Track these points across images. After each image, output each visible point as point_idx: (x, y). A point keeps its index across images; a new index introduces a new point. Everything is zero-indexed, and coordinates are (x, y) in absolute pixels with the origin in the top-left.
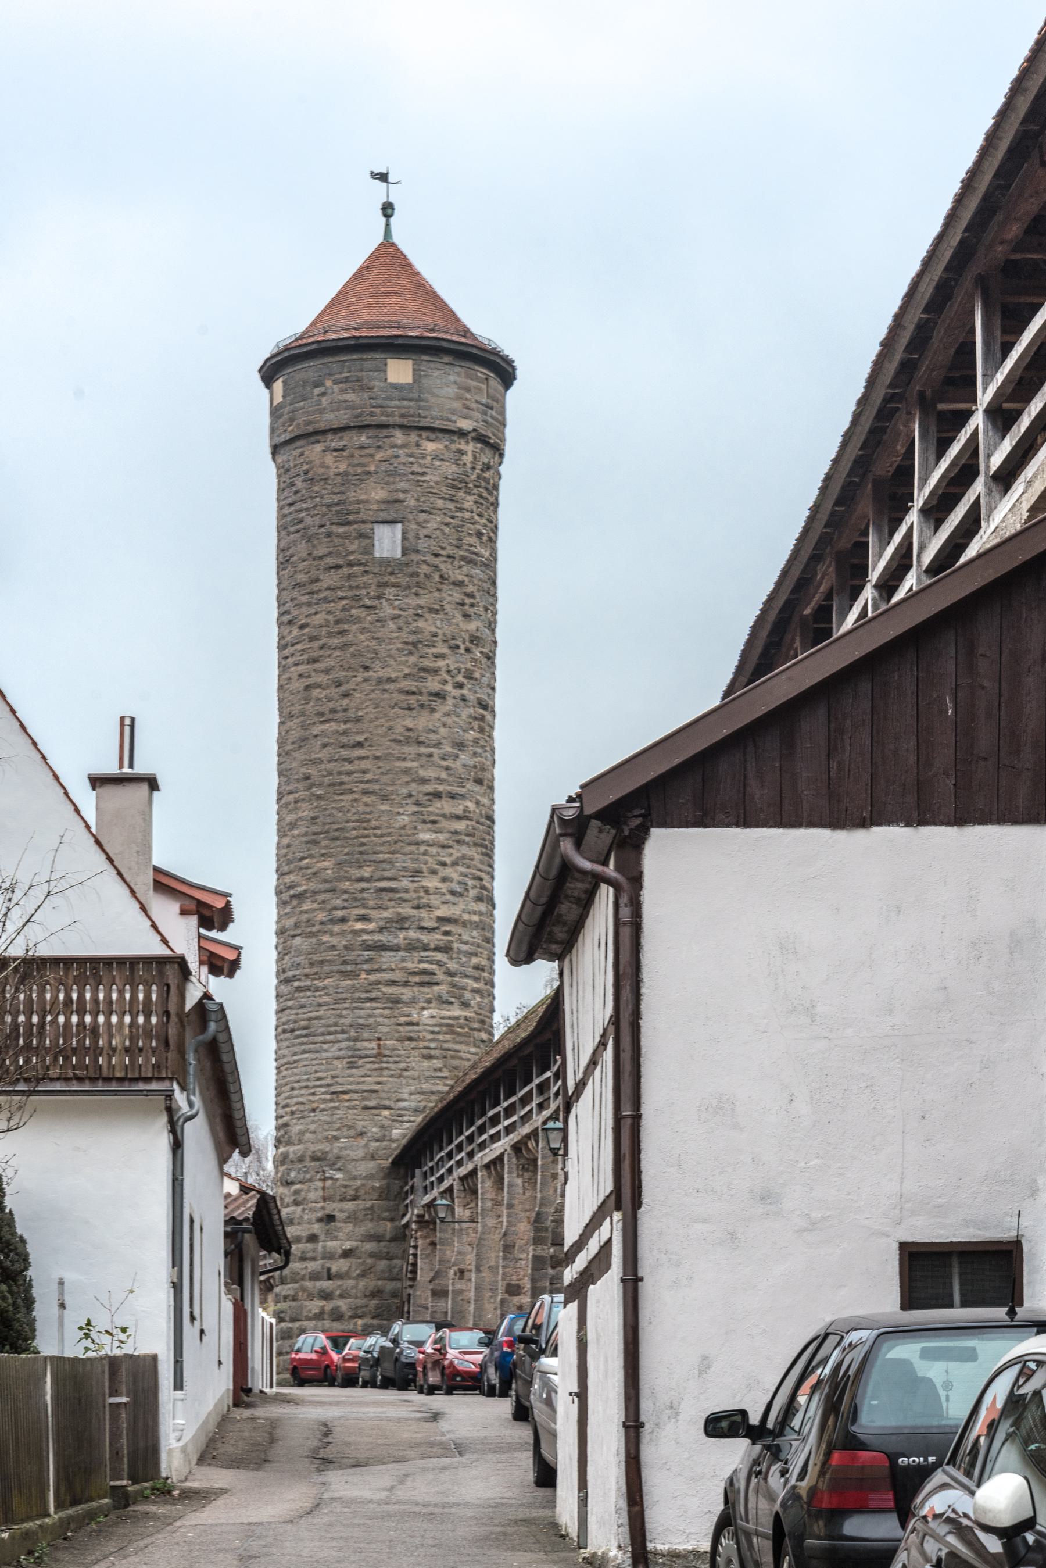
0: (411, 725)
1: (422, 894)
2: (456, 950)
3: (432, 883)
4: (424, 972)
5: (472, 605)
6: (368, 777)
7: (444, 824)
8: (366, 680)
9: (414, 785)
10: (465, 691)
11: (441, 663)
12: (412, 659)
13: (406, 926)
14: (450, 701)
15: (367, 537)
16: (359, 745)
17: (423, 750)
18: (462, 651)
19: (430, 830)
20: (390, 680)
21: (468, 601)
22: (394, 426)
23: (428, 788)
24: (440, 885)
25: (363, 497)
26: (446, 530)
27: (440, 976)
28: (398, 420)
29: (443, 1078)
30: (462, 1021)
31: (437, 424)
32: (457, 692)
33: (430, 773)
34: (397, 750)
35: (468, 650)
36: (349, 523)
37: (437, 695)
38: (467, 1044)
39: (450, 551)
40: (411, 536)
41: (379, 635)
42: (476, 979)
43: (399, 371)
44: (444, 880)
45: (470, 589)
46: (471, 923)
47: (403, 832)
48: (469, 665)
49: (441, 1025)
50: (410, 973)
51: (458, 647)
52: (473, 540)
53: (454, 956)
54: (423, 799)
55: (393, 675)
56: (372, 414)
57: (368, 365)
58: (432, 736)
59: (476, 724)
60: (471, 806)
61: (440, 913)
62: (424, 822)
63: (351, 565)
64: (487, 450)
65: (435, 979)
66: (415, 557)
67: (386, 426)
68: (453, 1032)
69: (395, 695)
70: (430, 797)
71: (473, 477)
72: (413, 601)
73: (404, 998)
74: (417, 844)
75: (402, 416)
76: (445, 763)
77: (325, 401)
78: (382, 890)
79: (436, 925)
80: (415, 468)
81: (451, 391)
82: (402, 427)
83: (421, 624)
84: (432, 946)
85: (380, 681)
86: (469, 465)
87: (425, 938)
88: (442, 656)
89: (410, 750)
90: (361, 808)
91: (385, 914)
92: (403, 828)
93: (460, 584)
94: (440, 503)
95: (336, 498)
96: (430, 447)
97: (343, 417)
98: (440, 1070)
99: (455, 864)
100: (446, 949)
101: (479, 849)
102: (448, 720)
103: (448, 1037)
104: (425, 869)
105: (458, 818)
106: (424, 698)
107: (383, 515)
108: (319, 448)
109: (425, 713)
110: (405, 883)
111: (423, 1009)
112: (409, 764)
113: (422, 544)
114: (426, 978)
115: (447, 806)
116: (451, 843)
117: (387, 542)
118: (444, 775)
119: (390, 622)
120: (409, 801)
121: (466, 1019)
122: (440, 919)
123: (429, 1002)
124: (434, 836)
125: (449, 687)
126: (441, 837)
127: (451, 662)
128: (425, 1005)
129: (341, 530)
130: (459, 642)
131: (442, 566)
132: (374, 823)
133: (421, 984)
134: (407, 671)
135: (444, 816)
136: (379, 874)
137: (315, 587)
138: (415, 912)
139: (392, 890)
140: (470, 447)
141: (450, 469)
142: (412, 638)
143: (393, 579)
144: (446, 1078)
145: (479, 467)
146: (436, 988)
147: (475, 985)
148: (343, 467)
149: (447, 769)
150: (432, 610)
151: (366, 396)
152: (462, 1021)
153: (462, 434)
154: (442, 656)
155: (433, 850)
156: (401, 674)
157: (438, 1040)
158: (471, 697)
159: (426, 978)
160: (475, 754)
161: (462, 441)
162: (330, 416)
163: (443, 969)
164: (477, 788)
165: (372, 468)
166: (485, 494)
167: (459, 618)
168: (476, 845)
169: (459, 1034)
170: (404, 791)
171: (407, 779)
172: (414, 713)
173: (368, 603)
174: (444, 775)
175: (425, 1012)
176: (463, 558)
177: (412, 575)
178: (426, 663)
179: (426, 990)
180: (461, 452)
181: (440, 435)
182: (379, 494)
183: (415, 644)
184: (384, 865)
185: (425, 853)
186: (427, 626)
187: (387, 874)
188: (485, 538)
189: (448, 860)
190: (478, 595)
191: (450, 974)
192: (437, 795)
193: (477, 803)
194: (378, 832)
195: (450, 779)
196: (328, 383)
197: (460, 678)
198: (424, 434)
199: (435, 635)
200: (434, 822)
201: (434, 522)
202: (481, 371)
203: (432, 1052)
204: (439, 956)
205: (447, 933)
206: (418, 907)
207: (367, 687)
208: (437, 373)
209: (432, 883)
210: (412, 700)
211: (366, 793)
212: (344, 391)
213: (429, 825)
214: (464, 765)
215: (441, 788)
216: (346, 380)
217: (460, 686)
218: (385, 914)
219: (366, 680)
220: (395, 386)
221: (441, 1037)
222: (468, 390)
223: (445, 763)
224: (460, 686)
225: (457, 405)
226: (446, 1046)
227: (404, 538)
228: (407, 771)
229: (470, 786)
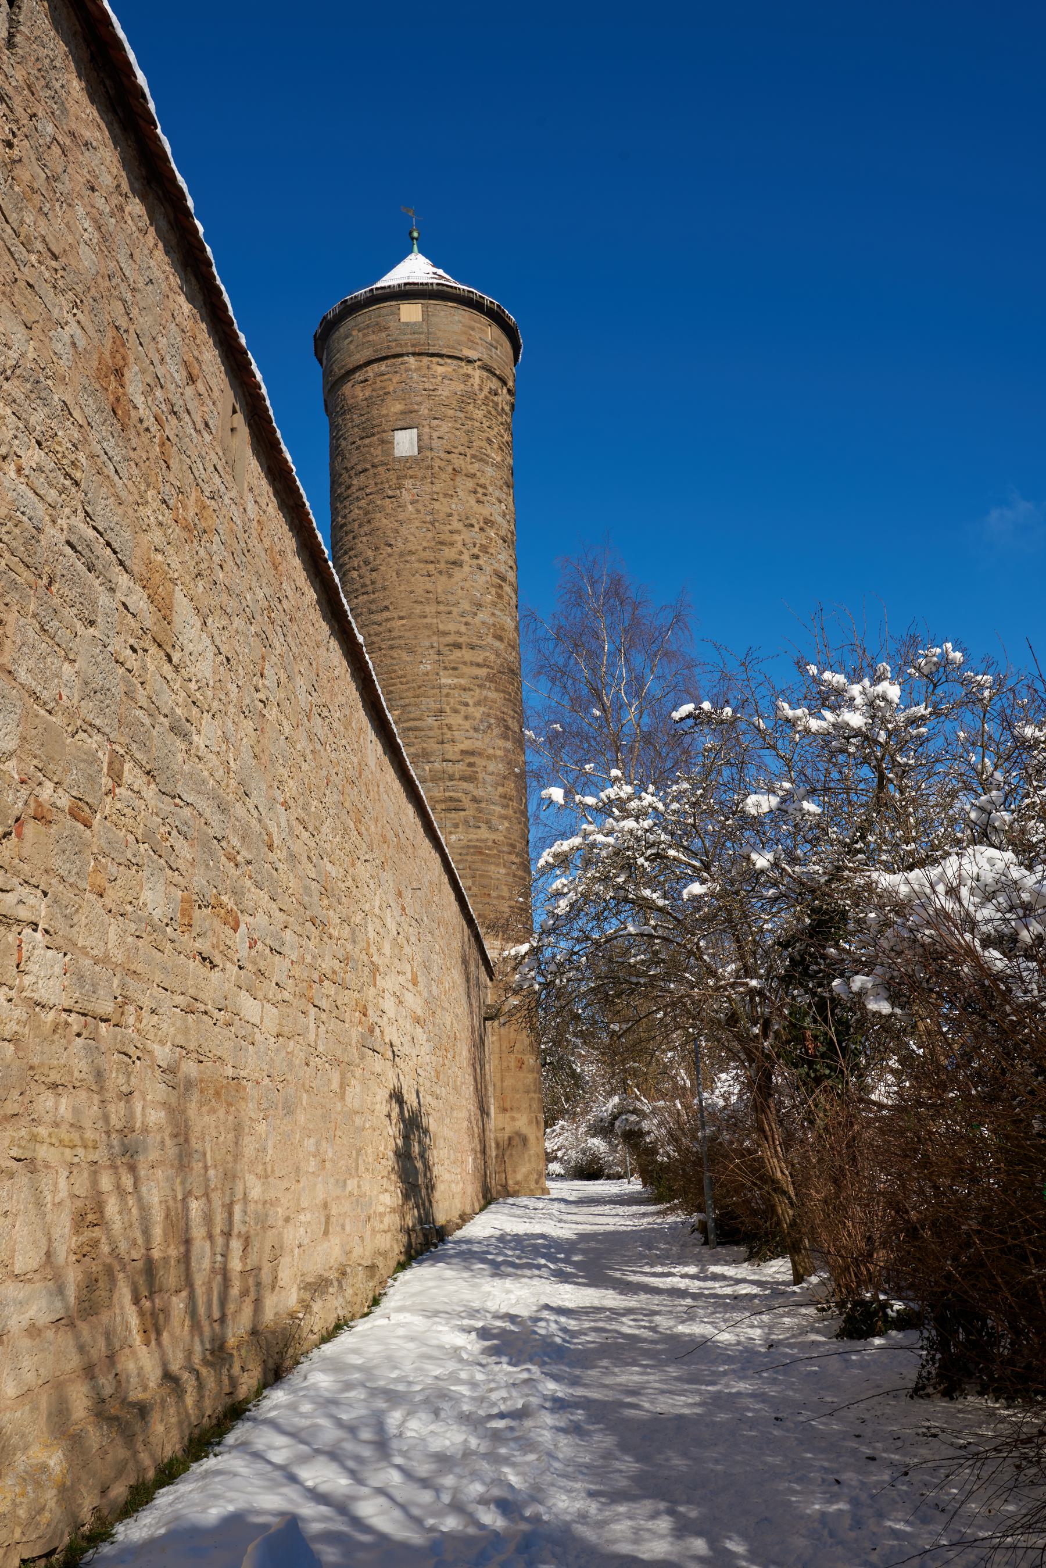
0: (430, 589)
1: (445, 730)
3: (455, 720)
4: (451, 799)
5: (485, 495)
6: (394, 634)
7: (465, 669)
8: (390, 555)
9: (435, 638)
10: (481, 562)
11: (456, 537)
12: (430, 535)
14: (466, 568)
15: (388, 444)
16: (387, 608)
17: (441, 608)
18: (477, 527)
19: (450, 676)
20: (411, 553)
21: (480, 490)
22: (407, 354)
23: (450, 639)
24: (461, 722)
25: (385, 412)
26: (458, 433)
27: (466, 802)
28: (411, 350)
30: (490, 844)
31: (444, 351)
32: (475, 561)
33: (451, 627)
34: (418, 609)
35: (482, 529)
36: (373, 435)
37: (454, 563)
38: (498, 865)
39: (461, 449)
40: (426, 437)
41: (400, 518)
42: (505, 807)
43: (411, 312)
44: (466, 718)
45: (482, 481)
46: (495, 756)
48: (484, 542)
51: (472, 526)
52: (484, 444)
54: (445, 650)
55: (413, 548)
56: (389, 347)
57: (385, 311)
58: (450, 598)
59: (493, 591)
60: (492, 657)
62: (445, 668)
63: (374, 466)
64: (494, 379)
66: (428, 453)
67: (402, 355)
69: (416, 565)
71: (482, 396)
72: (427, 488)
75: (413, 346)
76: (464, 620)
77: (352, 347)
78: (409, 729)
80: (426, 386)
81: (458, 328)
82: (414, 354)
83: (437, 505)
85: (401, 555)
86: (476, 387)
87: (449, 767)
88: (458, 532)
89: (430, 609)
90: (389, 661)
92: (427, 674)
93: (473, 476)
94: (451, 412)
95: (363, 419)
96: (440, 370)
97: (367, 354)
99: (478, 704)
100: (471, 779)
102: (467, 585)
103: (477, 858)
104: (448, 709)
105: (478, 665)
106: (442, 566)
107: (400, 424)
108: (350, 384)
109: (443, 578)
110: (430, 721)
111: (451, 833)
112: (428, 620)
113: (435, 443)
114: (453, 805)
115: (467, 655)
117: (405, 443)
118: (463, 629)
119: (410, 508)
120: (431, 651)
121: (494, 842)
123: (456, 826)
124: (456, 681)
125: (466, 557)
126: (462, 681)
127: (467, 535)
129: (367, 441)
130: (474, 521)
131: (455, 461)
133: (449, 810)
134: (425, 544)
135: (465, 663)
136: (405, 717)
137: (349, 492)
140: (478, 374)
141: (459, 387)
142: (429, 518)
143: (411, 472)
145: (486, 391)
146: (462, 813)
147: (503, 812)
148: (367, 393)
149: (466, 624)
150: (445, 495)
151: (384, 335)
152: (490, 844)
153: (470, 361)
154: (458, 532)
155: (456, 693)
156: (420, 548)
158: (488, 569)
159: (453, 805)
160: (493, 614)
161: (470, 367)
162: (358, 356)
164: (497, 643)
165: (391, 389)
166: (494, 412)
167: (472, 500)
168: (497, 690)
169: (488, 855)
170: (428, 644)
171: (427, 632)
172: (433, 579)
173: (390, 493)
174: (463, 629)
176: (473, 456)
177: (427, 468)
178: (442, 537)
179: (453, 815)
180: (469, 376)
181: (449, 361)
182: (398, 407)
183: (432, 523)
184: (410, 708)
185: (447, 695)
186: (442, 507)
187: (412, 716)
188: (496, 446)
189: (471, 703)
190: (491, 489)
191: (475, 800)
192: (458, 646)
193: (498, 655)
196: (355, 333)
197: (476, 551)
198: (435, 359)
199: (450, 515)
200: (455, 669)
201: (445, 427)
202: (484, 320)
204: (465, 785)
205: (470, 765)
206: (443, 743)
207: (392, 561)
208: (442, 314)
209: (455, 720)
210: (431, 567)
211: (392, 648)
212: (364, 335)
214: (483, 623)
215: (461, 640)
216: (368, 326)
217: (477, 557)
219: (390, 555)
220: (407, 324)
221: (469, 858)
222: (473, 329)
223: (464, 620)
224: (477, 557)
225: (464, 338)
227: (419, 440)
228: (428, 626)
229: (490, 639)
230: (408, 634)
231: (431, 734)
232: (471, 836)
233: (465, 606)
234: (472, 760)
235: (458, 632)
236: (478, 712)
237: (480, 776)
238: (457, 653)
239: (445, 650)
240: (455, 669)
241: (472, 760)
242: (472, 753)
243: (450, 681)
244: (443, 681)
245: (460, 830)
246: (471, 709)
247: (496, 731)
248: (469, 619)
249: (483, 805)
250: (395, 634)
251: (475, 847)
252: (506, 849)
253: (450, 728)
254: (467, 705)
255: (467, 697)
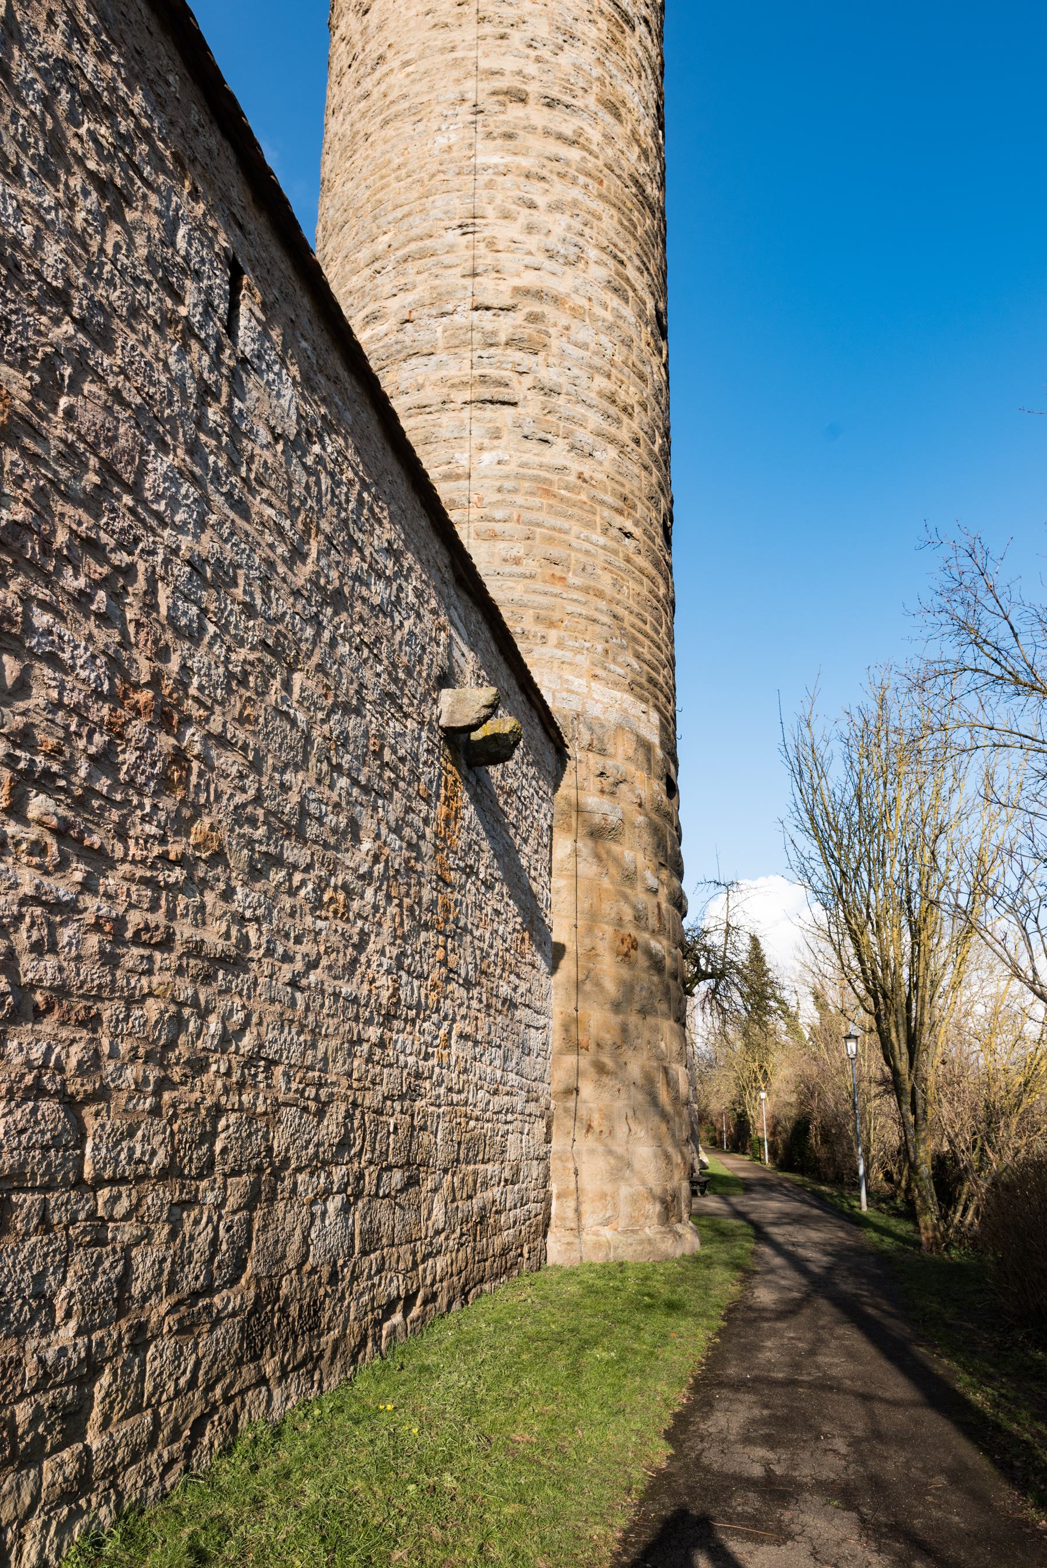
2: (554, 350)
9: (470, 84)
13: (449, 308)
17: (487, 29)
27: (519, 389)
29: (524, 576)
30: (572, 478)
33: (509, 64)
38: (589, 525)
44: (530, 229)
47: (446, 156)
49: (518, 477)
50: (453, 386)
53: (552, 360)
54: (489, 104)
61: (517, 282)
62: (489, 135)
65: (503, 394)
68: (547, 492)
70: (501, 98)
73: (444, 433)
74: (475, 171)
79: (508, 302)
84: (502, 338)
91: (409, 298)
98: (517, 561)
99: (556, 207)
101: (614, 211)
103: (536, 501)
104: (490, 212)
110: (453, 236)
116: (544, 173)
118: (532, 69)
121: (580, 476)
122: (516, 290)
124: (509, 159)
126: (527, 163)
128: (486, 442)
132: (397, 161)
138: (468, 281)
139: (422, 255)
144: (532, 577)
157: (512, 504)
159: (487, 393)
163: (528, 381)
170: (452, 95)
171: (455, 74)
174: (532, 69)
175: (487, 457)
185: (490, 185)
187: (414, 233)
189: (541, 201)
194: (403, 172)
195: (545, 77)
200: (509, 136)
203: (498, 527)
205: (534, 318)
206: (475, 275)
213: (499, 142)
214: (578, 68)
218: (409, 298)
221: (519, 499)
226: (527, 515)
230: (417, 87)
231: (447, 259)
232: (526, 458)
233: (542, 30)
234: (537, 307)
235: (520, 73)
236: (559, 224)
237: (555, 343)
238: (515, 111)
239: (489, 104)
240: (509, 136)
241: (537, 307)
242: (539, 295)
243: (495, 159)
244: (481, 160)
245: (502, 442)
246: (540, 217)
247: (600, 273)
248: (545, 53)
249: (561, 400)
250: (393, 95)
251: (536, 479)
252: (609, 499)
253: (491, 244)
254: (532, 206)
255: (535, 191)
